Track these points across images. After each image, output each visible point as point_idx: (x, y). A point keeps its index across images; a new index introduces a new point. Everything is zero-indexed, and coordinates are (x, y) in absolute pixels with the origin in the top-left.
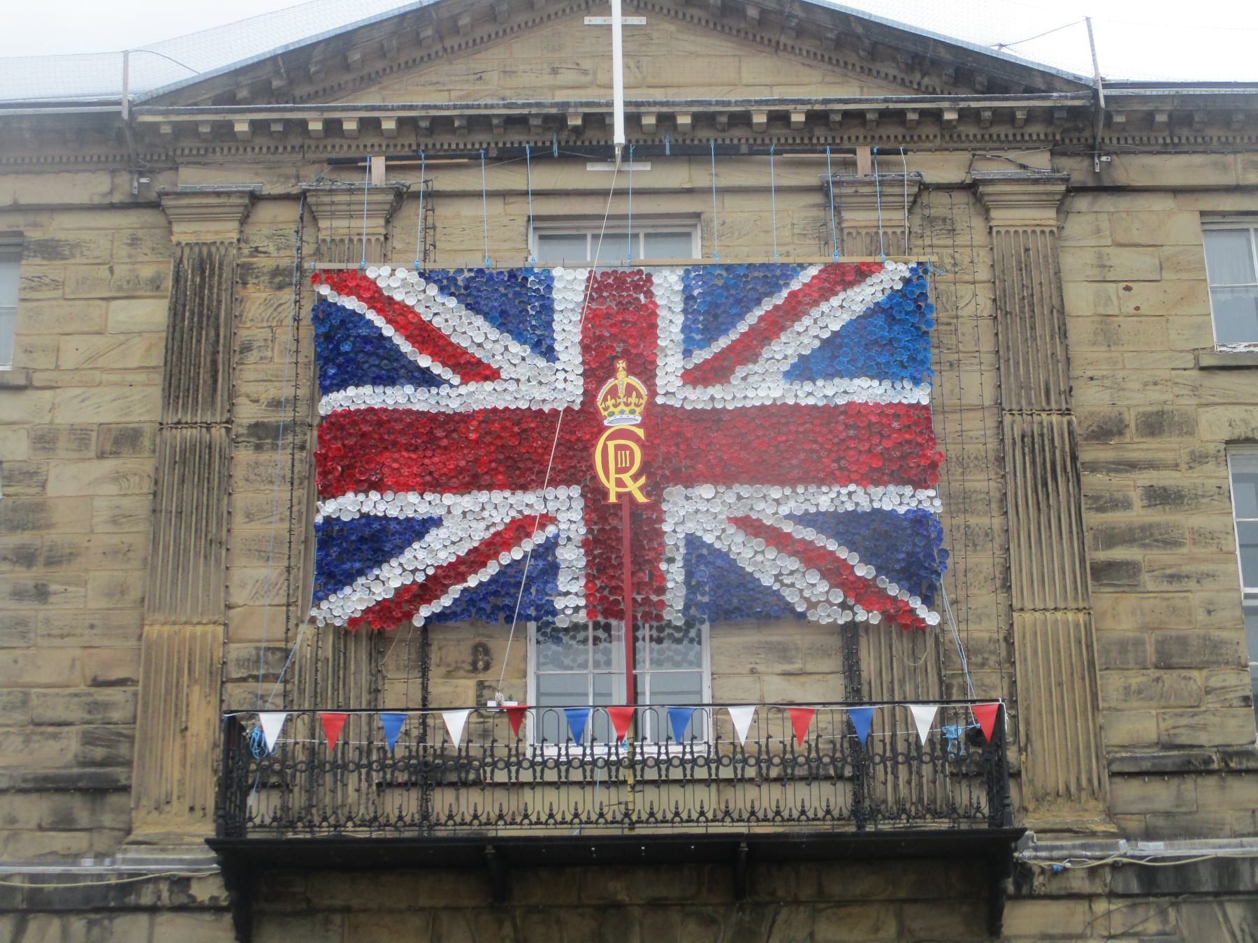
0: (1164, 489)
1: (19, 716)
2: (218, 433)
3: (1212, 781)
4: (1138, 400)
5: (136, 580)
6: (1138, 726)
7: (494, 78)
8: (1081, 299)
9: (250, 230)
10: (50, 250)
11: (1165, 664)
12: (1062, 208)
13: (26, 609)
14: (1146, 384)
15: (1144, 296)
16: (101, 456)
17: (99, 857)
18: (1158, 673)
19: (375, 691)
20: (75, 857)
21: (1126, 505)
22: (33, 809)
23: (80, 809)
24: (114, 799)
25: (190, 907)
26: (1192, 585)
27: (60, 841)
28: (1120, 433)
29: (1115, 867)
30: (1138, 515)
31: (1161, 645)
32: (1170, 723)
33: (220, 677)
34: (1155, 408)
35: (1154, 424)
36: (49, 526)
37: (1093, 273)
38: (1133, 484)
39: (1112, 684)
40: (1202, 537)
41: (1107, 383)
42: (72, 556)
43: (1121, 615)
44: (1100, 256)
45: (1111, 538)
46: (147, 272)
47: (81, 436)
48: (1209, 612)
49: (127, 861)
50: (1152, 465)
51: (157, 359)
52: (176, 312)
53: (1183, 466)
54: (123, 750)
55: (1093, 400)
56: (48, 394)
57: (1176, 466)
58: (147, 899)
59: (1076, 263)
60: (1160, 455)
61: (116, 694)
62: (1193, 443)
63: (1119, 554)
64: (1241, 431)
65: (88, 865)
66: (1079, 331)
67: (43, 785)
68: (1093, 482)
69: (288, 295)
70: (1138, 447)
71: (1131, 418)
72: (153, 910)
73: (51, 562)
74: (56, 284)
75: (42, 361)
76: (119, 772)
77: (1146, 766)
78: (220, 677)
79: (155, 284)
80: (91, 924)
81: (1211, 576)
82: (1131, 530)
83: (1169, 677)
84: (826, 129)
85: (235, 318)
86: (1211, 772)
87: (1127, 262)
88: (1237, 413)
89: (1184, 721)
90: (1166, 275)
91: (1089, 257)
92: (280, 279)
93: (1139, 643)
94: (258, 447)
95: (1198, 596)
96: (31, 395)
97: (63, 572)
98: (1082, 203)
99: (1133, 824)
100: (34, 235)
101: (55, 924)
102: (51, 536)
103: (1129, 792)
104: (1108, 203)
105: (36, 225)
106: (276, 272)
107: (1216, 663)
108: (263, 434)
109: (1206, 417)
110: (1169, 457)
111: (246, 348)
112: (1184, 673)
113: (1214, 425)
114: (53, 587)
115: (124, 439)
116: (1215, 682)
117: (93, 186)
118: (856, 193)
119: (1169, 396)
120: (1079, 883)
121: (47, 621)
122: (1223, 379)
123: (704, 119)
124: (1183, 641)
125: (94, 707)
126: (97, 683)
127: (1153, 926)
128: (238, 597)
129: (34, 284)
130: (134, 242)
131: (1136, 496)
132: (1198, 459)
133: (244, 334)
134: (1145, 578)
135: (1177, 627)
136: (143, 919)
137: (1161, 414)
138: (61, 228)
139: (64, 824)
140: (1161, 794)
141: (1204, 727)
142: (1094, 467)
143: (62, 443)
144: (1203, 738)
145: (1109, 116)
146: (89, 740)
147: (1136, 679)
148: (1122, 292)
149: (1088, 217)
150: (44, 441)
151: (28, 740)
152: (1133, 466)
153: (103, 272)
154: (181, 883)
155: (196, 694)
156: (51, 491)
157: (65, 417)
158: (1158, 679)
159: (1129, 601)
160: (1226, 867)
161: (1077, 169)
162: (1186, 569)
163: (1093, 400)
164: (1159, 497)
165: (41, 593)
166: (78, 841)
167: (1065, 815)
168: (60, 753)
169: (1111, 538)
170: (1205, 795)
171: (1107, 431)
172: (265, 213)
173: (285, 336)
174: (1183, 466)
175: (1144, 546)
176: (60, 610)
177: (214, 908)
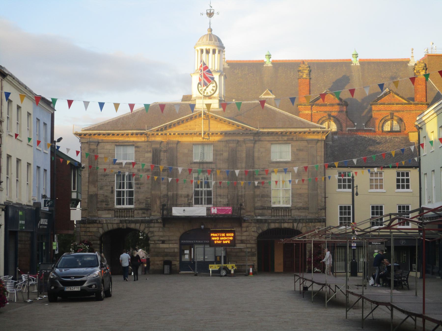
5: (150, 187)
6: (258, 204)
8: (256, 154)
11: (262, 197)
12: (254, 144)
13: (138, 190)
16: (145, 172)
17: (148, 217)
20: (145, 217)
22: (140, 212)
23: (145, 212)
24: (149, 211)
25: (158, 222)
27: (143, 215)
29: (254, 220)
33: (160, 198)
39: (256, 199)
40: (267, 183)
42: (143, 184)
46: (149, 150)
49: (152, 217)
51: (151, 161)
52: (153, 156)
54: (150, 205)
58: (154, 221)
59: (256, 150)
61: (149, 199)
65: (147, 218)
67: (141, 209)
69: (166, 153)
72: (154, 223)
73: (141, 184)
74: (139, 151)
76: (150, 208)
78: (160, 198)
79: (150, 151)
92: (165, 151)
98: (257, 142)
99: (257, 215)
101: (144, 225)
102: (140, 181)
103: (257, 211)
104: (260, 142)
106: (164, 151)
111: (161, 160)
120: (250, 221)
122: (272, 164)
125: (146, 201)
126: (147, 198)
127: (258, 226)
128: (162, 189)
129: (136, 152)
130: (147, 146)
139: (144, 213)
140: (260, 211)
146: (146, 204)
154: (157, 220)
155: (158, 200)
160: (266, 220)
161: (256, 138)
165: (140, 188)
166: (145, 215)
167: (249, 214)
168: (143, 206)
170: (265, 212)
173: (166, 159)
177: (161, 223)
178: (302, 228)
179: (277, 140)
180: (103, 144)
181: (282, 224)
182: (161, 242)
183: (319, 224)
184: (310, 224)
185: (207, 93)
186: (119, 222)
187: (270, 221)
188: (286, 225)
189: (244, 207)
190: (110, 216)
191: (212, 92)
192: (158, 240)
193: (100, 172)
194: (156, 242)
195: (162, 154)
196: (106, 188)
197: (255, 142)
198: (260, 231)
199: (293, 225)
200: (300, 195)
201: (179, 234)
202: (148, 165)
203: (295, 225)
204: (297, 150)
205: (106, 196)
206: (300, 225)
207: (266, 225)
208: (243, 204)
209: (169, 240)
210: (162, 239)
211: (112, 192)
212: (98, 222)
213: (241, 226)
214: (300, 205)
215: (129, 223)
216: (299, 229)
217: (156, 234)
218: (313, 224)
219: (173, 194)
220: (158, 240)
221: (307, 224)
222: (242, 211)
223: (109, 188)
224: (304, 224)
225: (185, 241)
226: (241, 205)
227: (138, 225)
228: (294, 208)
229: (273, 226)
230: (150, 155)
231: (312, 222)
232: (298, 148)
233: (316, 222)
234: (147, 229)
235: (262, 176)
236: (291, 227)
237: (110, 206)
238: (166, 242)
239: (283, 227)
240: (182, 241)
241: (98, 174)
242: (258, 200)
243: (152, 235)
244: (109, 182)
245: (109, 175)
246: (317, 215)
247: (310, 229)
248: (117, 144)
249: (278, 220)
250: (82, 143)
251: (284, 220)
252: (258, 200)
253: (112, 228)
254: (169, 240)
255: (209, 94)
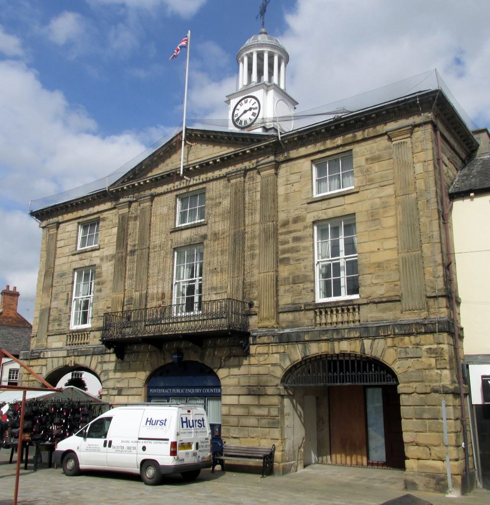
0: (297, 237)
1: (97, 316)
2: (124, 253)
3: (303, 312)
4: (293, 214)
6: (286, 300)
7: (170, 165)
8: (281, 190)
9: (131, 209)
10: (104, 219)
13: (98, 294)
14: (295, 210)
15: (296, 187)
16: (110, 261)
18: (293, 285)
19: (146, 305)
21: (287, 242)
26: (301, 261)
28: (288, 224)
30: (291, 245)
31: (293, 278)
32: (294, 298)
34: (297, 216)
35: (296, 220)
36: (102, 277)
37: (285, 183)
38: (289, 237)
39: (282, 289)
40: (305, 248)
41: (286, 211)
42: (105, 282)
43: (285, 271)
44: (287, 178)
45: (284, 252)
47: (107, 257)
48: (305, 268)
50: (295, 231)
53: (302, 230)
55: (282, 216)
56: (102, 250)
57: (300, 231)
60: (297, 228)
62: (305, 224)
63: (286, 256)
64: (316, 219)
66: (281, 199)
68: (281, 238)
70: (292, 227)
71: (291, 220)
73: (102, 284)
74: (105, 226)
75: (102, 243)
77: (287, 310)
80: (102, 357)
81: (306, 258)
82: (289, 249)
83: (295, 286)
84: (225, 161)
85: (128, 228)
86: (302, 310)
87: (294, 178)
88: (315, 214)
89: (297, 297)
90: (302, 179)
91: (284, 179)
93: (288, 278)
94: (131, 256)
95: (303, 264)
96: (101, 250)
97: (104, 285)
98: (284, 165)
99: (284, 325)
100: (101, 217)
104: (290, 164)
105: (102, 215)
107: (306, 281)
108: (133, 252)
109: (308, 216)
110: (299, 228)
111: (130, 234)
112: (298, 285)
113: (310, 218)
114: (102, 289)
115: (113, 257)
116: (305, 286)
117: (108, 205)
118: (232, 176)
119: (300, 212)
121: (101, 296)
123: (201, 165)
124: (298, 276)
131: (290, 240)
132: (305, 227)
133: (129, 232)
134: (291, 261)
135: (298, 273)
136: (108, 355)
137: (298, 217)
138: (105, 215)
140: (290, 316)
141: (302, 299)
142: (281, 234)
143: (104, 259)
144: (301, 301)
145: (283, 142)
147: (287, 287)
148: (291, 187)
149: (284, 170)
150: (102, 259)
151: (98, 321)
152: (290, 232)
153: (111, 222)
156: (103, 270)
157: (105, 254)
158: (292, 287)
159: (287, 267)
162: (300, 257)
163: (282, 216)
164: (296, 239)
169: (284, 252)
171: (285, 224)
172: (134, 205)
174: (302, 230)
175: (291, 253)
176: (103, 294)
178: (384, 351)
179: (322, 148)
180: (64, 224)
181: (336, 344)
182: (115, 392)
183: (429, 337)
184: (407, 338)
185: (246, 122)
186: (66, 356)
187: (307, 338)
188: (345, 347)
189: (257, 310)
190: (59, 345)
191: (253, 118)
192: (114, 389)
193: (57, 270)
194: (111, 392)
195: (131, 223)
196: (61, 297)
197: (277, 165)
198: (287, 364)
199: (363, 345)
200: (379, 265)
201: (143, 375)
202: (111, 250)
203: (367, 343)
204: (367, 160)
205: (60, 310)
206: (380, 343)
207: (300, 346)
208: (255, 302)
209: (129, 388)
210: (119, 385)
211: (68, 302)
212: (42, 356)
213: (247, 354)
214: (380, 292)
215: (78, 356)
216: (377, 354)
217: (111, 375)
218: (412, 338)
219: (141, 295)
220: (114, 389)
221: (397, 340)
222: (253, 320)
223: (64, 296)
224: (389, 341)
225: (155, 391)
226: (251, 305)
227: (89, 358)
228: (365, 301)
229: (314, 349)
230: (115, 230)
231: (409, 334)
232: (369, 156)
233: (421, 333)
234: (99, 366)
235: (293, 235)
236: (358, 351)
237: (62, 328)
238: (123, 393)
239: (337, 352)
240: (151, 390)
241: (55, 274)
242: (285, 291)
243: (106, 377)
244: (65, 285)
245: (66, 274)
246: (424, 314)
247: (407, 353)
248: (80, 220)
249: (326, 331)
250: (43, 228)
251: (337, 331)
252: (285, 291)
253: (57, 367)
254: (129, 388)
255: (249, 122)
